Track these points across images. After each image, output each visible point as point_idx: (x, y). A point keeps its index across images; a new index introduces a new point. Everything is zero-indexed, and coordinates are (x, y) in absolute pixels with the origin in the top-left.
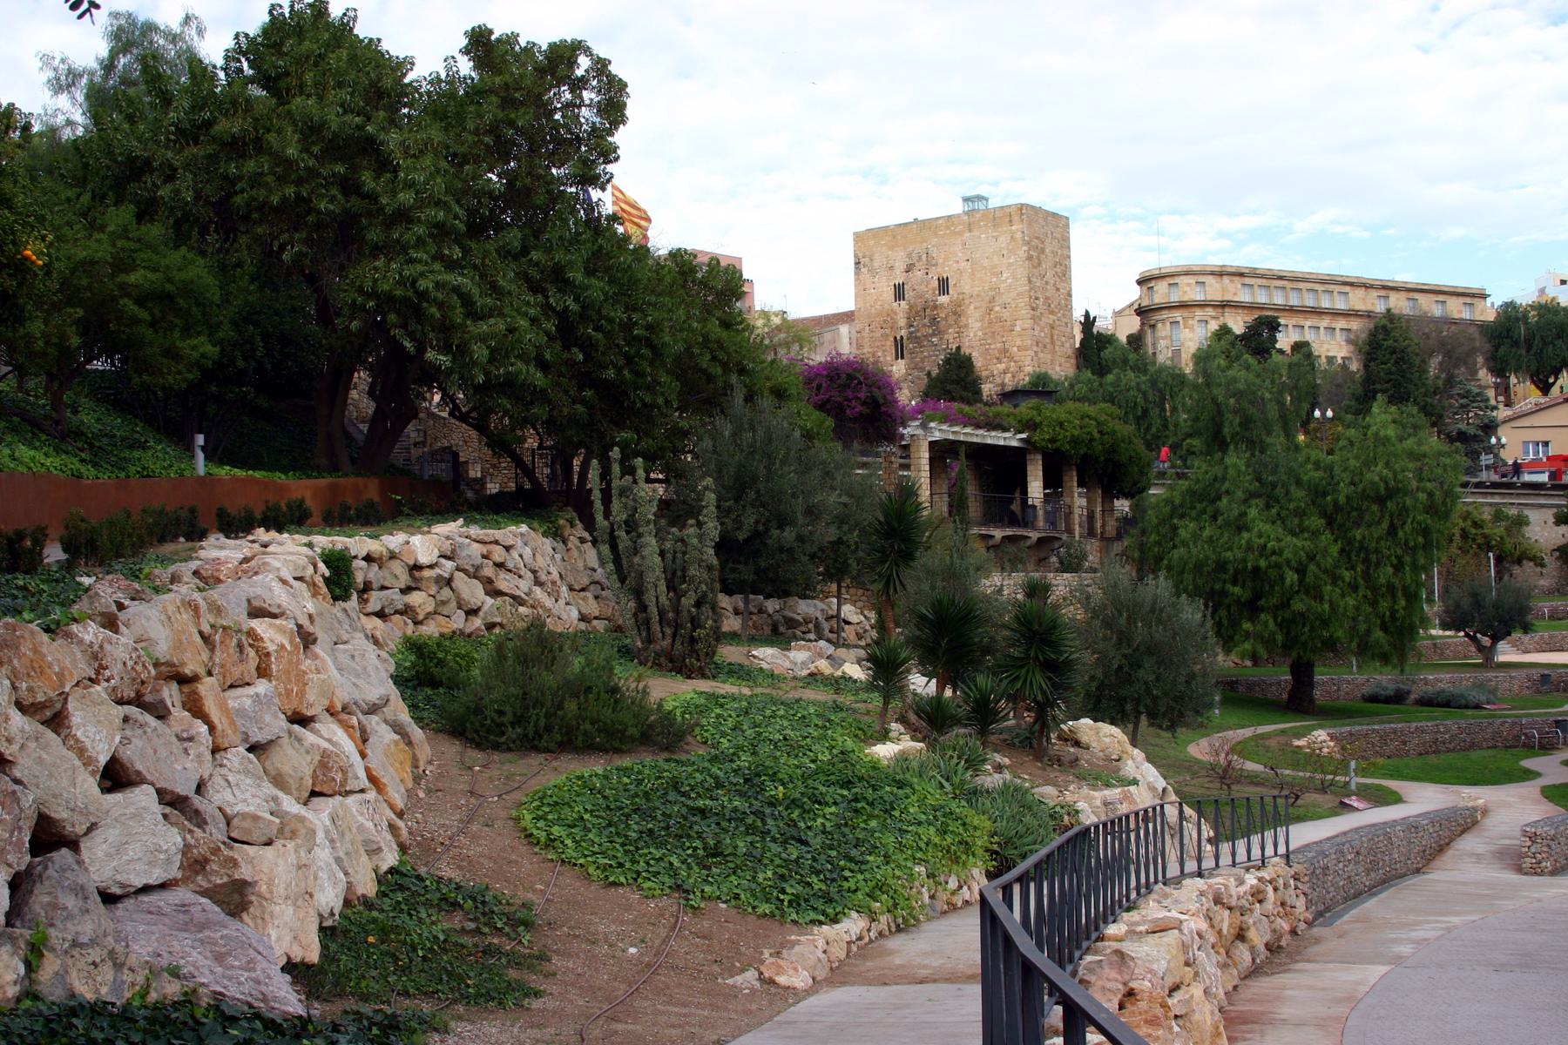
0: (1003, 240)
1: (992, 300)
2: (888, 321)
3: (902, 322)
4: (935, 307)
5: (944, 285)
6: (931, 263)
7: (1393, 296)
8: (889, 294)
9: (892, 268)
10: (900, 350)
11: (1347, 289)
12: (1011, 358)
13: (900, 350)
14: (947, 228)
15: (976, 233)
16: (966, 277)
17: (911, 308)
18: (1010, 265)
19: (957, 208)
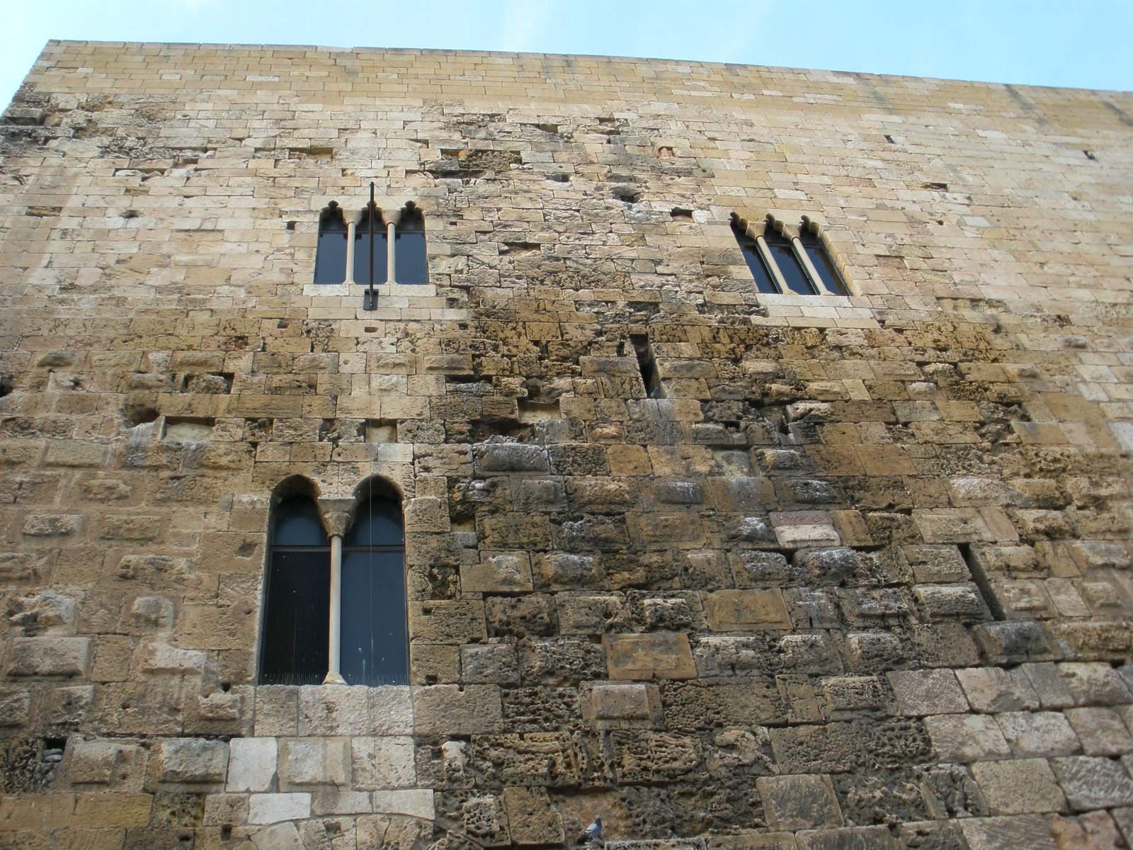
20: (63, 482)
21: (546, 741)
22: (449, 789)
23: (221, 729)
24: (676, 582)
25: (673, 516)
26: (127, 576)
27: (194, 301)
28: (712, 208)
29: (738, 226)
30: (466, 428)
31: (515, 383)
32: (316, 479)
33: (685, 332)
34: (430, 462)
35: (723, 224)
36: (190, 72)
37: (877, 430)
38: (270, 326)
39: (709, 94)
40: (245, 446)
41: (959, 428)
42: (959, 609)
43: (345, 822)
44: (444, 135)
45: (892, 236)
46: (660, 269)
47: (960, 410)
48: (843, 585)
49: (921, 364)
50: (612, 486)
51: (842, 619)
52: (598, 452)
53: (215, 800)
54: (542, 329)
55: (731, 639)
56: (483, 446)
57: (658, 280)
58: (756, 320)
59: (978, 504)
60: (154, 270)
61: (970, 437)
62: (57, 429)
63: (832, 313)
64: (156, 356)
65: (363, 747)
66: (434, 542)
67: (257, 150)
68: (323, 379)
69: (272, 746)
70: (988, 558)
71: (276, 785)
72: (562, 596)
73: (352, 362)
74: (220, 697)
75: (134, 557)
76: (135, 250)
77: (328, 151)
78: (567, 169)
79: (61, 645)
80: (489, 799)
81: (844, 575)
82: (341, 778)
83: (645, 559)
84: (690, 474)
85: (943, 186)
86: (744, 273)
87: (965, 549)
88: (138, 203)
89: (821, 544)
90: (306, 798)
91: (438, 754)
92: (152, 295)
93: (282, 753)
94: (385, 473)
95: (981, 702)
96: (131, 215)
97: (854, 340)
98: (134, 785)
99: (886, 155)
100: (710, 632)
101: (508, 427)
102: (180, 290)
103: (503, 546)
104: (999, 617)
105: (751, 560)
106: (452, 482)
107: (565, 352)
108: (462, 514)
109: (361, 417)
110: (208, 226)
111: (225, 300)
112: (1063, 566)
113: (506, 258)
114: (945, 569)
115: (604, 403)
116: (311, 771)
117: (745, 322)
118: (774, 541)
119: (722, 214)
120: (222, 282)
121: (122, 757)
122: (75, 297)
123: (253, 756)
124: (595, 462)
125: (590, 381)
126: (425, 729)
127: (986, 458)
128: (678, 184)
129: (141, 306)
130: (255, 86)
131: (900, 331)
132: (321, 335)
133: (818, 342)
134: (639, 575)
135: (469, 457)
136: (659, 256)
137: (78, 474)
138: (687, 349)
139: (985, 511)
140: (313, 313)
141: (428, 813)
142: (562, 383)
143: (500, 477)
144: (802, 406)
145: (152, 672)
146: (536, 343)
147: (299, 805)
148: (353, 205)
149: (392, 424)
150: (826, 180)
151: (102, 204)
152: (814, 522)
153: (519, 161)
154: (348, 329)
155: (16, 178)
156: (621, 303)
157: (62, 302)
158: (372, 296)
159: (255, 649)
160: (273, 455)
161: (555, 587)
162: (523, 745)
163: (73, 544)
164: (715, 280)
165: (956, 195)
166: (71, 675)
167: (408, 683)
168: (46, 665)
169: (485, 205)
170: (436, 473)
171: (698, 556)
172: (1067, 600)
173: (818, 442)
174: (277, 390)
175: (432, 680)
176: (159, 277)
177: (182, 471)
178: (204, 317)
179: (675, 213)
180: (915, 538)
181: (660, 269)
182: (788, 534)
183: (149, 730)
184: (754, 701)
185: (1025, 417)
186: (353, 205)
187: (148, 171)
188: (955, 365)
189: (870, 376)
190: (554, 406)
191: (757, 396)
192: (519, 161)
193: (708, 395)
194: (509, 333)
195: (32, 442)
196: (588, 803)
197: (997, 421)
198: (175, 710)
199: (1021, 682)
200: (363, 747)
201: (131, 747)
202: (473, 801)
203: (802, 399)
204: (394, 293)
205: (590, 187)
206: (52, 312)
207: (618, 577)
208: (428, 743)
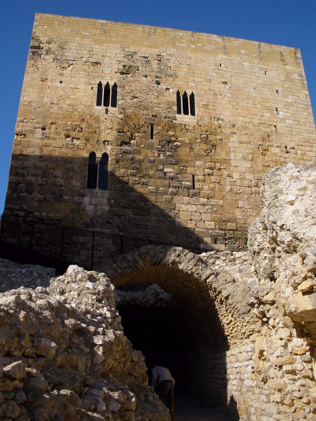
4: (172, 126)
5: (186, 104)
14: (193, 43)
15: (235, 58)
16: (223, 101)
18: (288, 105)
20: (57, 150)
21: (125, 201)
22: (111, 206)
23: (83, 195)
24: (147, 177)
25: (149, 165)
26: (68, 169)
27: (75, 109)
28: (174, 88)
29: (178, 93)
30: (120, 143)
31: (128, 134)
32: (96, 152)
33: (160, 124)
34: (114, 150)
35: (175, 93)
36: (69, 29)
37: (188, 150)
38: (89, 116)
39: (184, 45)
40: (85, 145)
41: (202, 151)
42: (188, 187)
43: (98, 210)
44: (124, 59)
45: (209, 99)
46: (160, 106)
47: (204, 147)
48: (172, 180)
49: (201, 135)
50: (141, 158)
51: (169, 186)
52: (140, 150)
53: (82, 206)
54: (135, 121)
55: (152, 188)
56: (122, 148)
57: (158, 109)
58: (174, 121)
59: (199, 167)
60: (67, 99)
61: (203, 153)
62: (54, 139)
63: (188, 120)
64: (69, 123)
65: (101, 199)
66: (113, 166)
67: (85, 62)
68: (97, 130)
69: (89, 198)
70: (196, 178)
71: (89, 204)
72: (130, 177)
73: (102, 127)
74: (82, 191)
75: (69, 166)
76: (63, 94)
77: (99, 63)
78: (148, 74)
79: (60, 181)
80: (116, 209)
81: (172, 179)
82: (98, 204)
83: (143, 172)
84: (154, 156)
85: (227, 83)
86: (175, 108)
87: (193, 176)
88: (63, 79)
89: (170, 172)
90: (93, 206)
91: (110, 201)
92: (67, 107)
93: (90, 200)
94: (107, 152)
95: (185, 202)
96: (61, 82)
97: (191, 128)
98: (72, 203)
99: (218, 71)
100: (150, 186)
101: (126, 143)
102: (72, 105)
103: (123, 168)
104: (194, 188)
105: (159, 174)
106: (117, 155)
107: (139, 127)
108: (117, 162)
109: (103, 140)
110: (76, 87)
111: (81, 108)
112: (208, 181)
113: (132, 100)
114: (188, 179)
115: (143, 140)
116: (94, 203)
117: (172, 122)
118: (163, 171)
119: (175, 90)
120: (79, 104)
121: (70, 199)
122: (54, 106)
123: (86, 200)
124: (139, 152)
125: (141, 134)
126: (109, 197)
127: (204, 158)
128: (169, 80)
129: (65, 110)
130: (84, 37)
131: (200, 126)
132: (97, 119)
133: (184, 128)
134: (142, 175)
135: (120, 150)
136: (160, 102)
137: (59, 149)
138: (160, 128)
139: (200, 169)
140: (96, 114)
141: (108, 209)
142: (137, 134)
143: (124, 154)
144: (176, 143)
145: (73, 186)
146: (134, 124)
147: (92, 207)
148: (104, 83)
149: (108, 141)
150: (201, 80)
151: (55, 78)
152: (171, 168)
153: (138, 70)
154: (102, 118)
155: (37, 68)
156: (151, 115)
157: (51, 107)
158: (107, 110)
159: (87, 183)
160: (89, 147)
161: (129, 176)
162: (122, 201)
163: (60, 163)
164: (169, 110)
165: (228, 86)
166: (62, 186)
167: (107, 190)
168: (58, 184)
169: (130, 85)
170: (114, 153)
171: (151, 173)
172: (206, 187)
173: (177, 151)
174: (90, 133)
175: (111, 190)
176: (68, 102)
177: (75, 149)
178: (77, 113)
179: (167, 89)
180: (186, 173)
181: (160, 106)
182: (166, 170)
183: (73, 195)
184: (153, 198)
185: (216, 149)
186: (104, 83)
187: (63, 68)
188: (208, 135)
189: (190, 137)
190: (135, 139)
191: (169, 140)
192: (138, 70)
193: (161, 139)
194: (130, 122)
195: (51, 142)
196: (129, 210)
197: (210, 150)
198: (76, 192)
199: (192, 200)
200: (101, 199)
201: (71, 197)
202: (114, 208)
203: (177, 141)
204: (110, 108)
205: (151, 80)
206: (50, 110)
207: (139, 175)
208: (109, 199)
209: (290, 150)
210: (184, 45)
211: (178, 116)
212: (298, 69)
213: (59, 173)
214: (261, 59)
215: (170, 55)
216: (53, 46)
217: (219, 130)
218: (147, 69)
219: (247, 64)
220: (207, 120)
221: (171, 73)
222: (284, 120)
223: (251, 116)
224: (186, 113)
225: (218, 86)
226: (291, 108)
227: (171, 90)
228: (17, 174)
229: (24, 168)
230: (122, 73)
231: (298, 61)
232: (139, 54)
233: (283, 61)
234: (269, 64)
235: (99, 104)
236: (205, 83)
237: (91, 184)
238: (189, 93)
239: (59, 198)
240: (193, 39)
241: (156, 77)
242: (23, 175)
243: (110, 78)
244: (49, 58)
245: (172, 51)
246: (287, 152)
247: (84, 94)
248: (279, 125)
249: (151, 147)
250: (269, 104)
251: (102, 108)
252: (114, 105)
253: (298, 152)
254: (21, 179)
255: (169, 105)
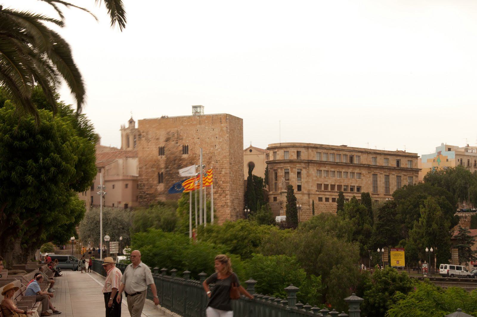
0: (217, 130)
1: (210, 158)
2: (155, 164)
3: (163, 166)
4: (181, 159)
5: (185, 149)
6: (179, 138)
7: (379, 157)
8: (156, 152)
9: (158, 139)
10: (160, 178)
11: (360, 154)
12: (219, 187)
13: (160, 178)
15: (203, 126)
17: (168, 159)
18: (220, 143)
19: (189, 112)
23: (157, 186)
29: (183, 146)
39: (186, 124)
79: (151, 182)
86: (182, 152)
123: (158, 187)
124: (171, 170)
132: (159, 161)
133: (184, 159)
150: (190, 139)
171: (174, 177)
176: (151, 155)
204: (162, 156)
209: (218, 162)
210: (186, 124)
211: (183, 155)
212: (226, 125)
213: (151, 179)
214: (212, 123)
215: (181, 130)
216: (144, 134)
217: (195, 158)
218: (174, 138)
219: (207, 127)
220: (192, 155)
221: (181, 138)
222: (217, 149)
223: (206, 150)
224: (185, 154)
225: (196, 140)
226: (221, 144)
227: (181, 145)
228: (140, 181)
229: (142, 179)
230: (167, 141)
231: (227, 120)
232: (171, 132)
233: (221, 122)
234: (215, 125)
235: (159, 155)
236: (192, 140)
237: (159, 182)
238: (187, 145)
239: (151, 187)
240: (189, 120)
241: (177, 141)
242: (142, 181)
243: (162, 145)
244: (144, 139)
245: (182, 127)
246: (217, 162)
247: (155, 151)
248: (216, 152)
249: (174, 168)
250: (213, 144)
251: (160, 156)
252: (164, 155)
253: (221, 162)
254: (142, 183)
255: (181, 151)
